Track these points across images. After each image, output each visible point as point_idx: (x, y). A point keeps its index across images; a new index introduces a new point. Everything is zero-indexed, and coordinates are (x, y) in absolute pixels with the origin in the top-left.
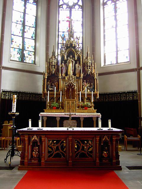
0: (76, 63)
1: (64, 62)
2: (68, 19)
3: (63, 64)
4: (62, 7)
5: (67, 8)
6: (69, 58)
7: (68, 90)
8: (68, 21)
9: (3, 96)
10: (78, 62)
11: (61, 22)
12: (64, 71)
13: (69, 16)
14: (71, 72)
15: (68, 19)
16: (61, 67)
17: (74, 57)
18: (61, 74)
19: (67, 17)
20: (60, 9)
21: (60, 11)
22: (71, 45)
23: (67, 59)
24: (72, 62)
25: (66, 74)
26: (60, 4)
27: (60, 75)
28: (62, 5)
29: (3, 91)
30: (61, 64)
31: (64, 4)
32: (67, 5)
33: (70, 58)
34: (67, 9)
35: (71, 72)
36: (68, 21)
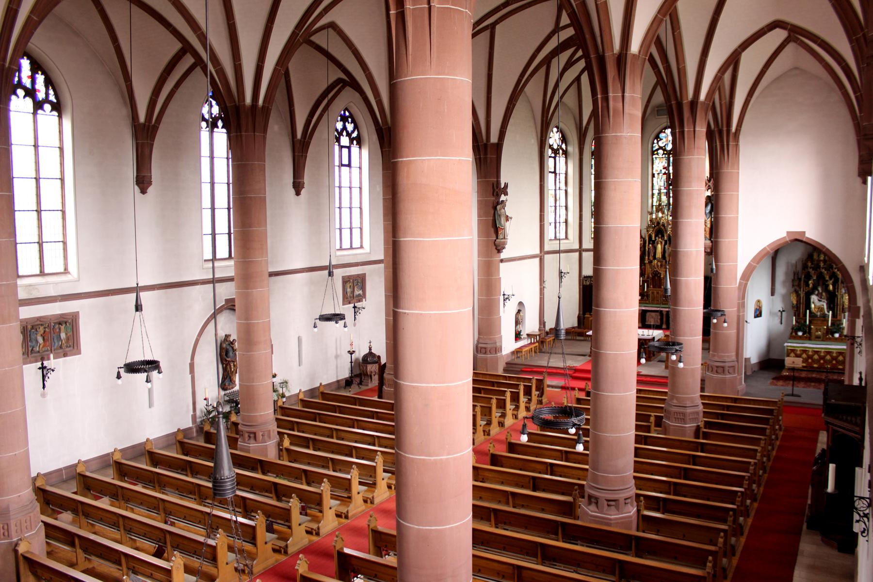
0: (666, 244)
1: (651, 242)
2: (664, 171)
3: (650, 245)
4: (657, 154)
5: (664, 154)
6: (657, 238)
7: (653, 277)
8: (665, 174)
9: (584, 282)
10: (668, 242)
11: (656, 175)
12: (652, 254)
13: (666, 165)
14: (659, 254)
15: (664, 171)
16: (649, 249)
17: (663, 236)
18: (649, 257)
19: (664, 168)
20: (654, 156)
21: (654, 159)
22: (658, 223)
23: (656, 239)
24: (661, 243)
25: (655, 258)
26: (654, 149)
27: (647, 257)
28: (657, 150)
29: (584, 277)
30: (649, 244)
31: (660, 148)
32: (664, 150)
33: (659, 238)
34: (664, 156)
35: (659, 254)
36: (665, 174)
